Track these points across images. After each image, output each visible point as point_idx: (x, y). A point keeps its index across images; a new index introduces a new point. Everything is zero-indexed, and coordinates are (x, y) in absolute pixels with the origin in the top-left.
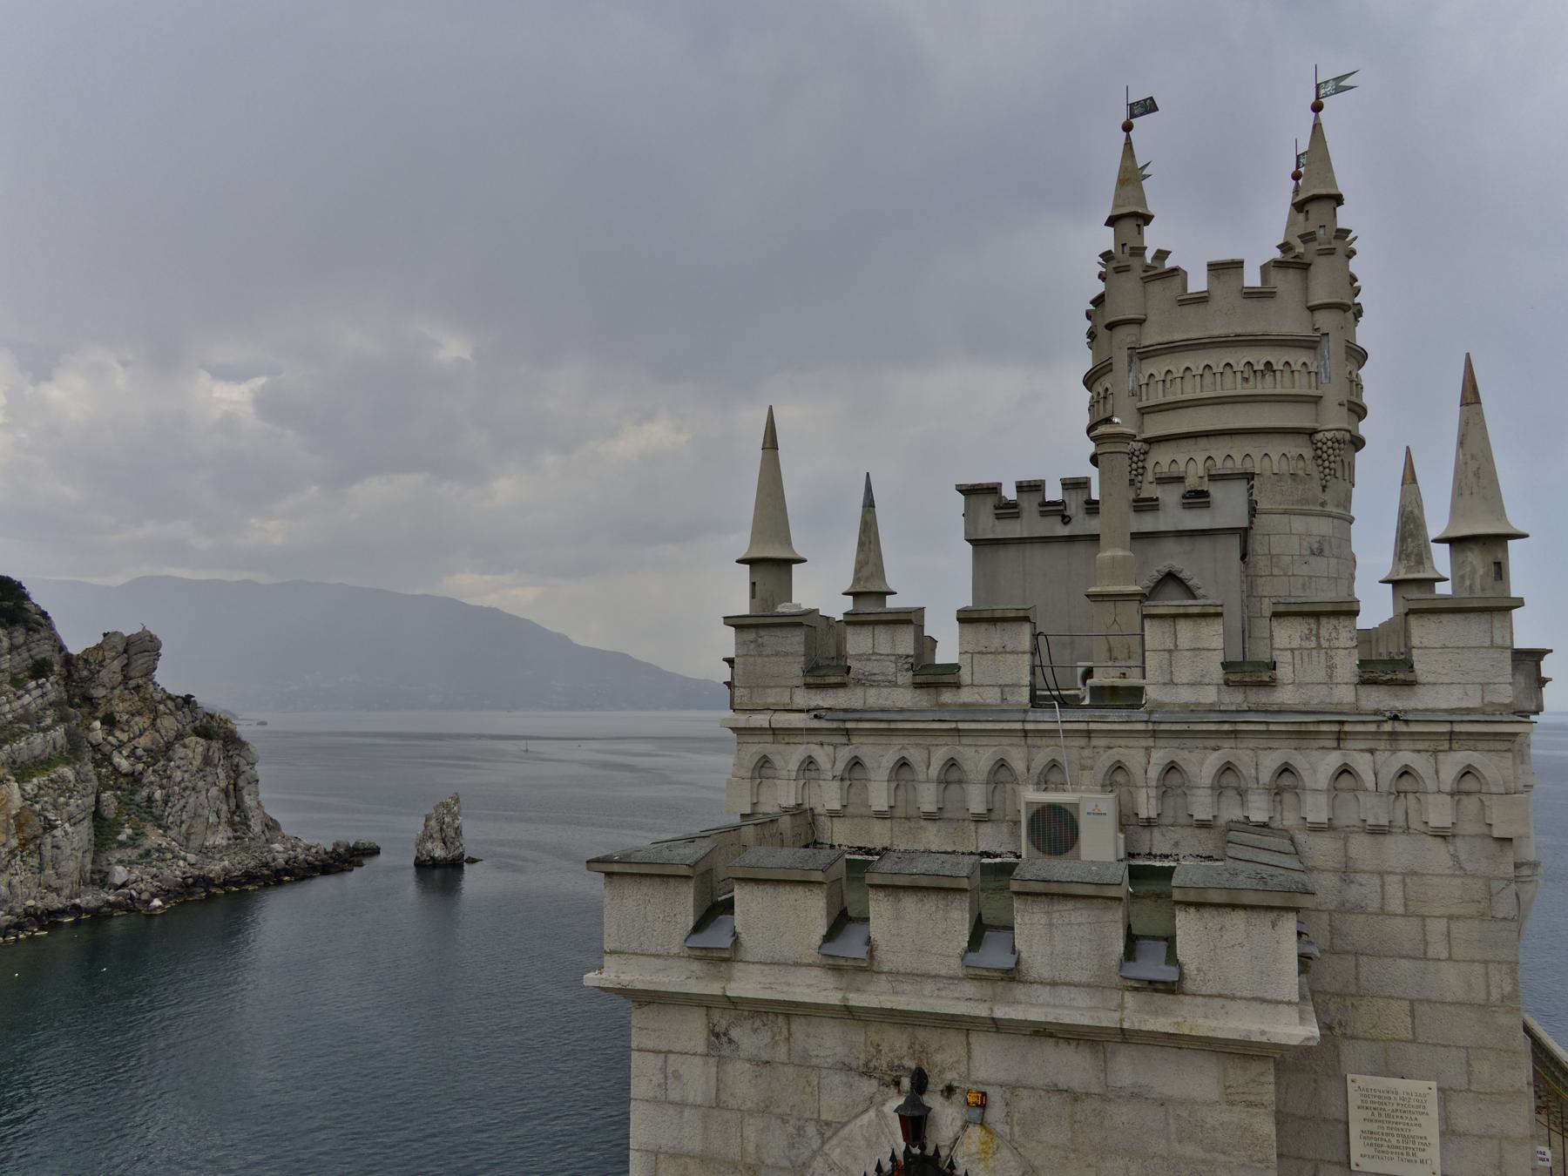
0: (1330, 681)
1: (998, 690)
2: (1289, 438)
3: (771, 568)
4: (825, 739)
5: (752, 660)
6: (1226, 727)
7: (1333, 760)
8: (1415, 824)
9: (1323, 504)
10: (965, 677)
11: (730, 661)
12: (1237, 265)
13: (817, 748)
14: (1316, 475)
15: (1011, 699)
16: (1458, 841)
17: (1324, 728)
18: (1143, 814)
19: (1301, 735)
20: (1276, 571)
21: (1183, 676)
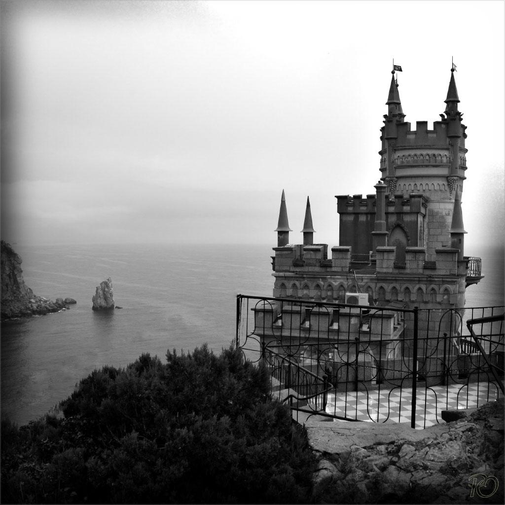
0: (418, 268)
1: (341, 268)
2: (440, 179)
3: (283, 234)
4: (298, 279)
5: (279, 259)
6: (394, 278)
7: (417, 286)
8: (434, 301)
9: (450, 199)
10: (333, 265)
11: (273, 258)
12: (425, 123)
13: (296, 281)
14: (448, 190)
15: (344, 270)
16: (443, 305)
17: (416, 279)
18: (374, 298)
19: (410, 281)
20: (434, 221)
21: (385, 266)
